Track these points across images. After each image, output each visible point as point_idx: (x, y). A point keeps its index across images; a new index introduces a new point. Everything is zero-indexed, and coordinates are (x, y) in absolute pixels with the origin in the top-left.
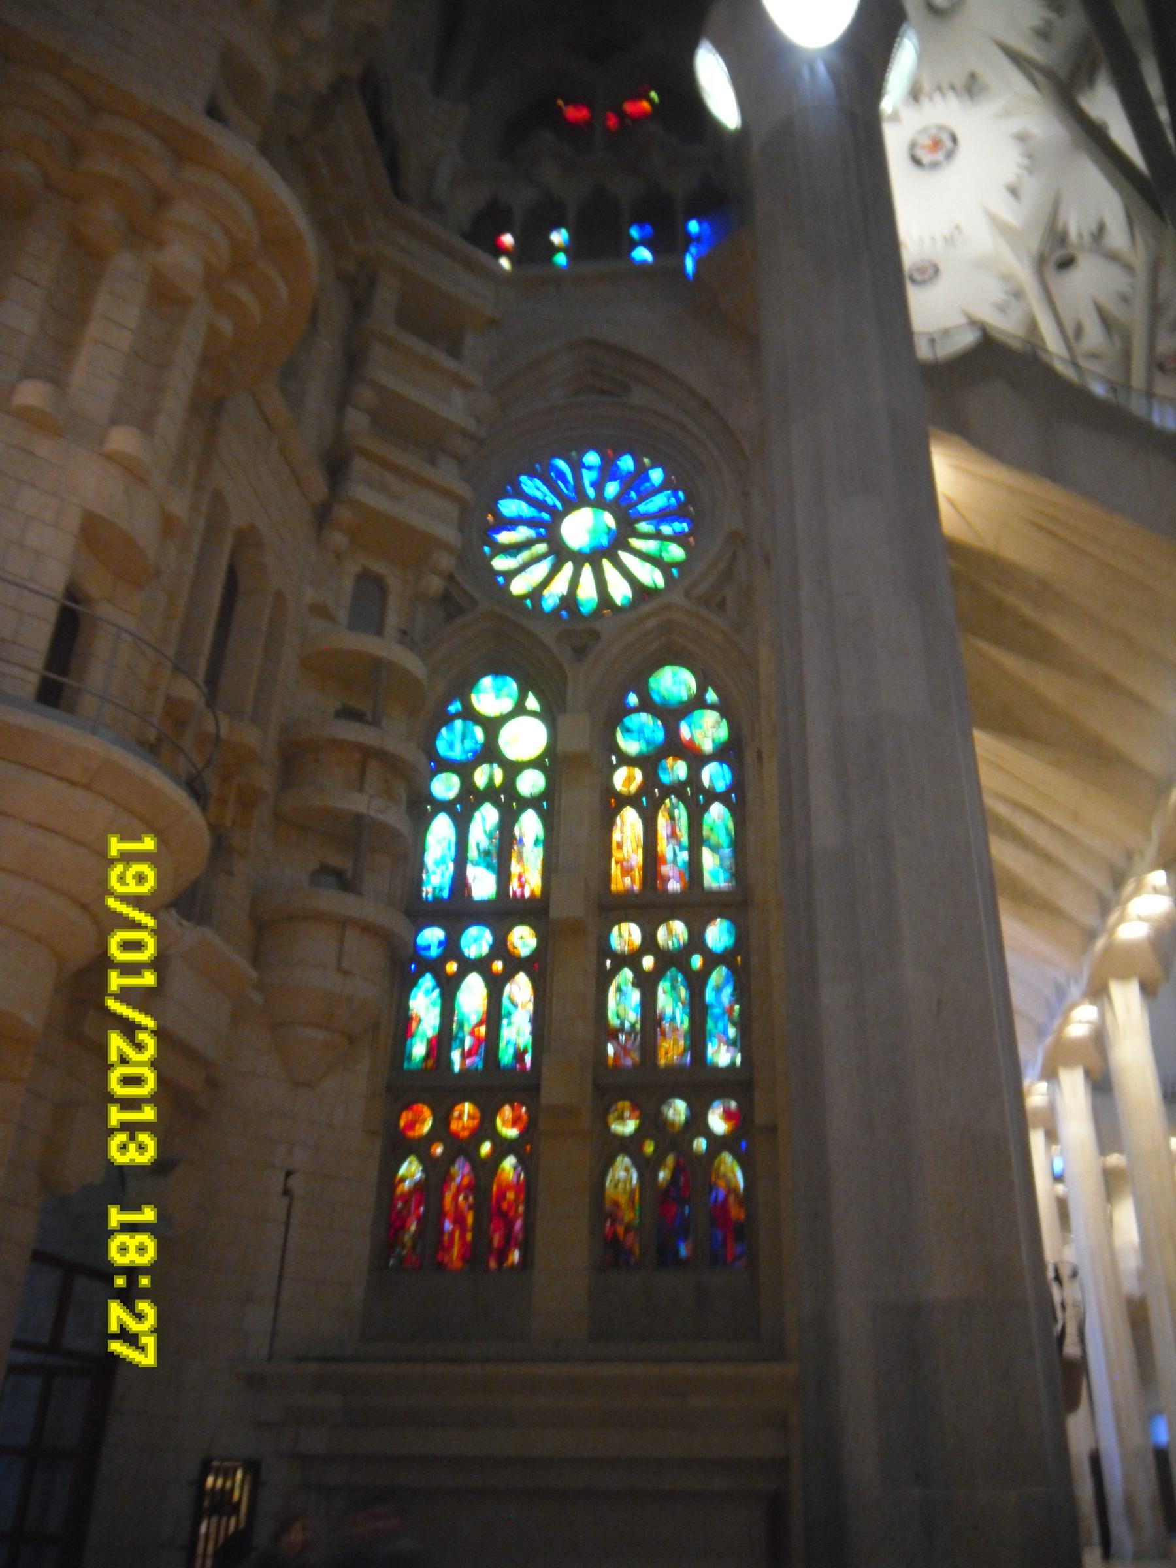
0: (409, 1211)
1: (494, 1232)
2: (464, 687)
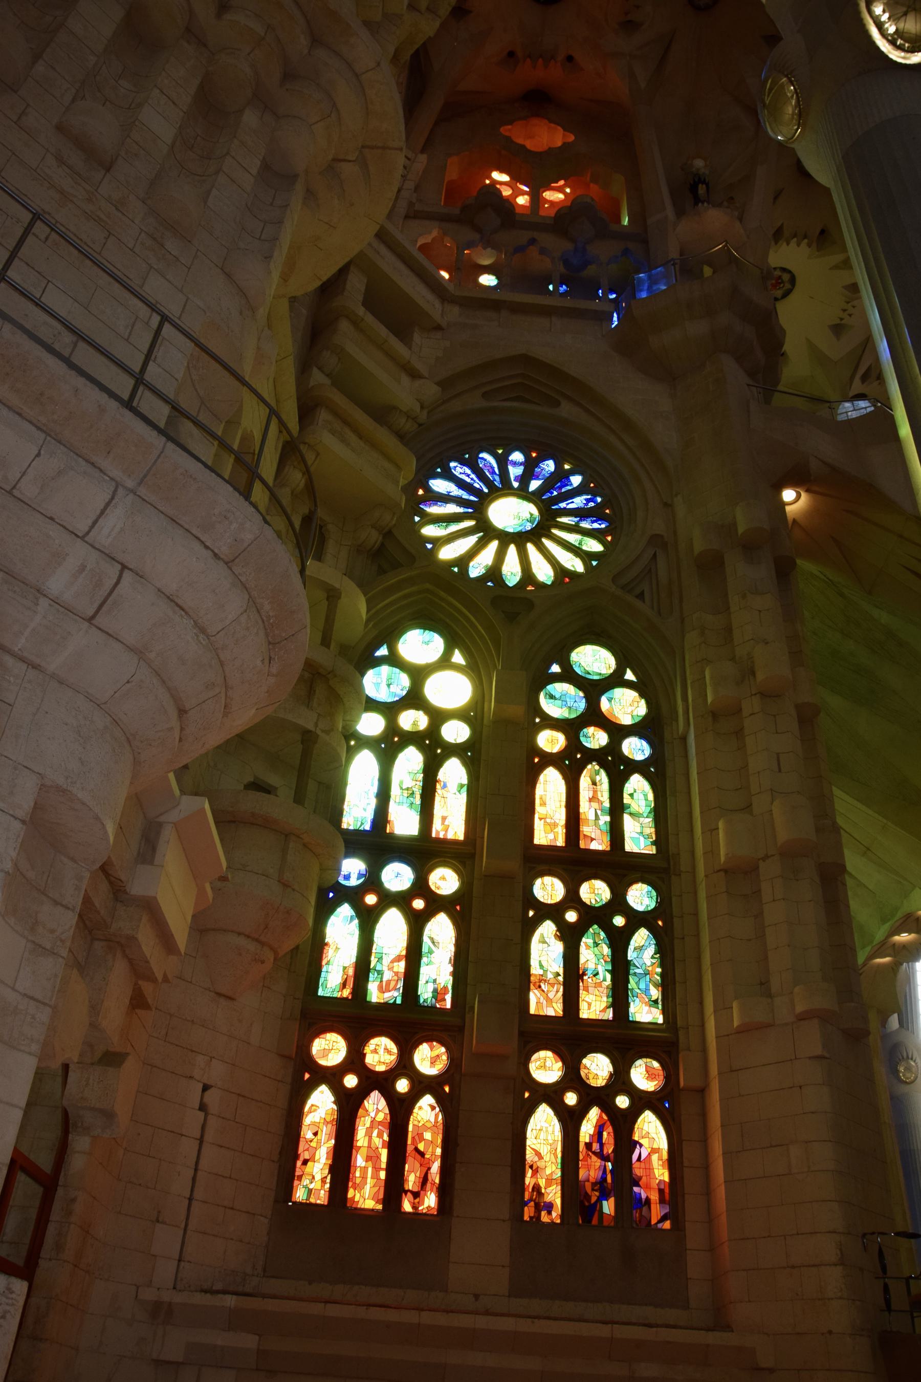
0: (319, 1142)
1: (410, 1172)
2: (391, 636)
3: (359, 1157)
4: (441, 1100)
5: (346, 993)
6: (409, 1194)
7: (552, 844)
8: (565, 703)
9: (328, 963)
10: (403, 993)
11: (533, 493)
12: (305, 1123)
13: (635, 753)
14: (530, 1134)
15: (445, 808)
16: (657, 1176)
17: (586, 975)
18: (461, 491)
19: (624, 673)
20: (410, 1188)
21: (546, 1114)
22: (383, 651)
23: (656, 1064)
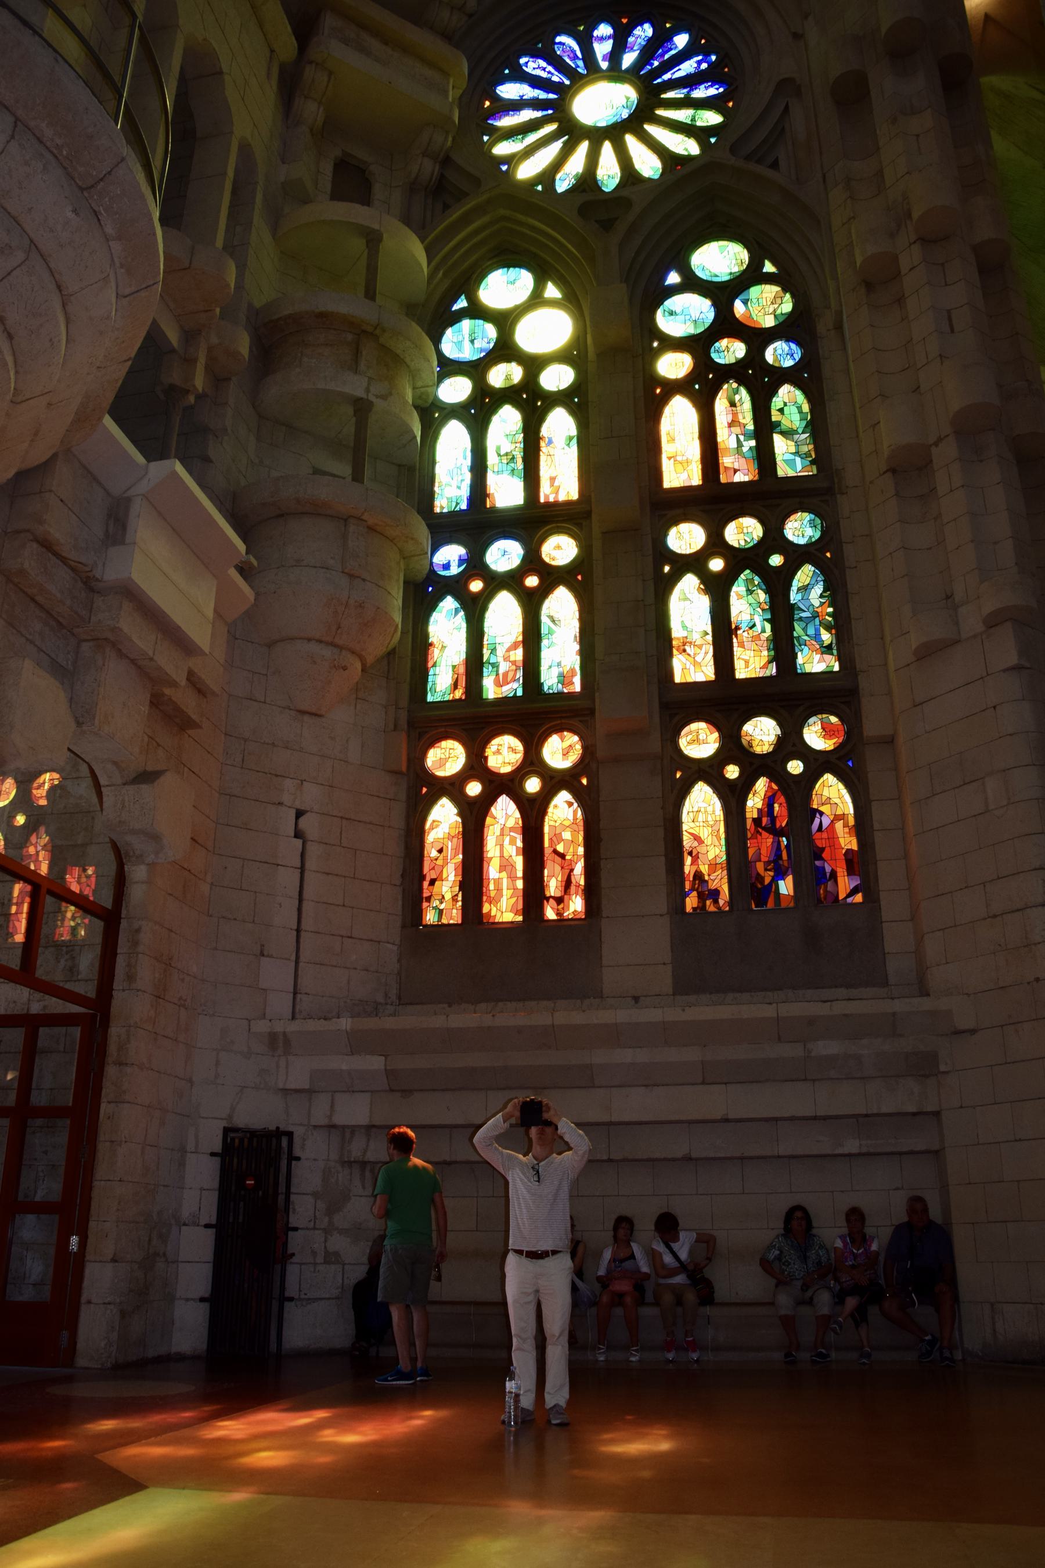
0: (445, 859)
1: (550, 876)
5: (459, 694)
6: (551, 900)
7: (685, 485)
9: (434, 665)
10: (523, 683)
11: (627, 70)
12: (428, 842)
13: (782, 359)
14: (686, 818)
16: (843, 846)
17: (739, 629)
19: (763, 265)
20: (553, 895)
21: (703, 793)
22: (462, 303)
23: (834, 719)
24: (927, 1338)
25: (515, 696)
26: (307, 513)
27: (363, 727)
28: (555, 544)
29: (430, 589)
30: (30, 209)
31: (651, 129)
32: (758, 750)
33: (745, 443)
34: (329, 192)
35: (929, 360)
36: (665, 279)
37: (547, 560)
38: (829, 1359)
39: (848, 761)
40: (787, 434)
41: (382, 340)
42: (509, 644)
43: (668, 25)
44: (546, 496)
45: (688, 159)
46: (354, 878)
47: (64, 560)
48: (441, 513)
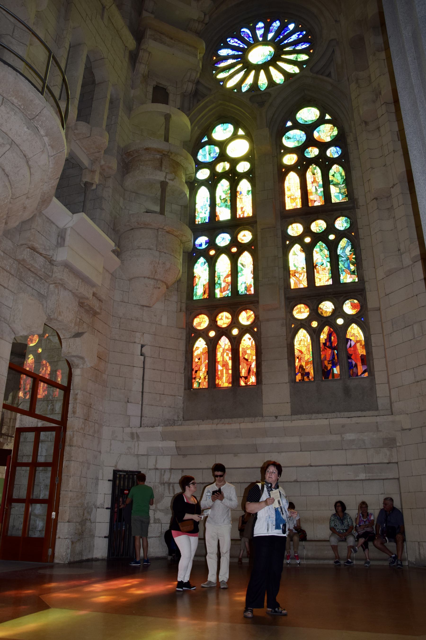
0: (201, 362)
1: (242, 368)
3: (219, 365)
4: (253, 335)
5: (206, 296)
6: (243, 378)
8: (295, 139)
9: (196, 285)
10: (231, 291)
11: (270, 40)
15: (242, 203)
16: (360, 353)
18: (234, 51)
20: (243, 375)
21: (303, 333)
22: (206, 139)
23: (356, 301)
24: (393, 556)
25: (228, 296)
26: (142, 228)
27: (168, 311)
28: (243, 235)
29: (194, 254)
30: (11, 129)
31: (280, 64)
32: (325, 315)
33: (318, 190)
34: (151, 99)
35: (390, 152)
36: (286, 125)
37: (240, 241)
38: (352, 564)
39: (362, 318)
40: (336, 185)
41: (171, 157)
42: (225, 276)
43: (286, 21)
44: (240, 215)
45: (295, 74)
46: (165, 371)
47: (41, 254)
48: (198, 224)
